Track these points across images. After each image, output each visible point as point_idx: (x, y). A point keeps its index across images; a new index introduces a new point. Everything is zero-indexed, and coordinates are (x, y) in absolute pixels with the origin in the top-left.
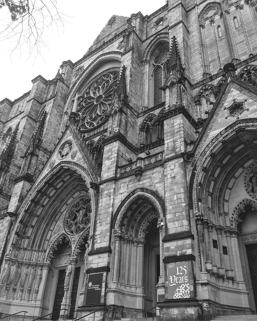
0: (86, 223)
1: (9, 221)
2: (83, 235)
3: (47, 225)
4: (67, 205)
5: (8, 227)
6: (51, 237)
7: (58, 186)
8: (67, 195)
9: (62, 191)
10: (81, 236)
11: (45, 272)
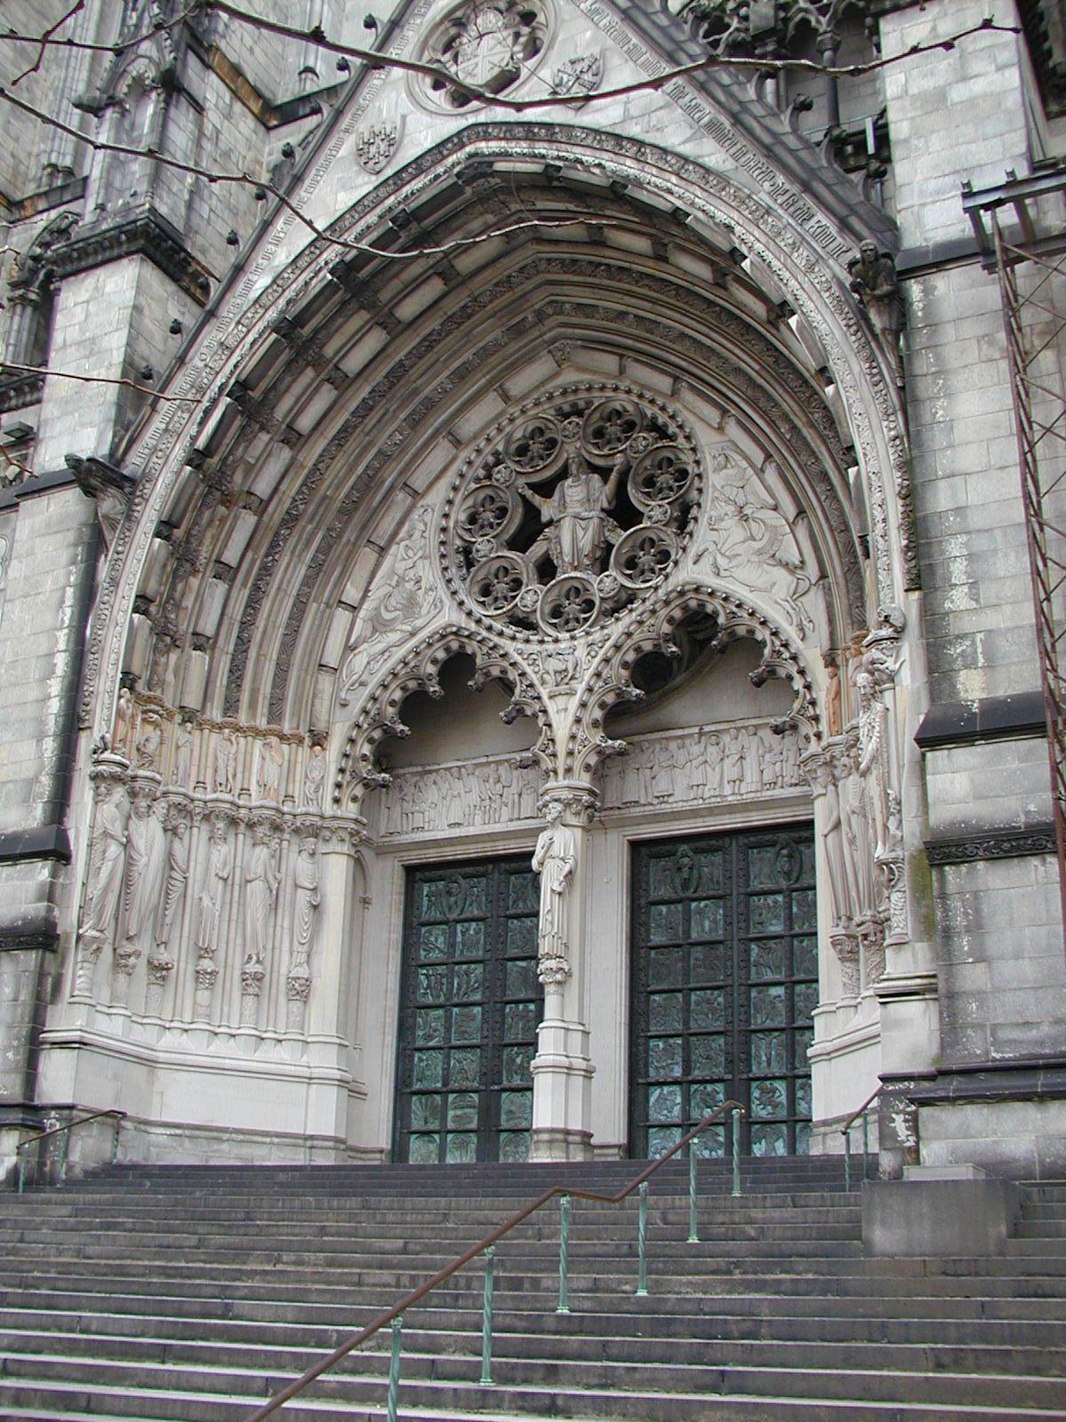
0: (631, 563)
1: (75, 525)
2: (630, 642)
3: (317, 568)
4: (457, 443)
5: (73, 563)
6: (350, 648)
7: (407, 310)
8: (461, 375)
9: (430, 343)
10: (617, 647)
11: (337, 869)
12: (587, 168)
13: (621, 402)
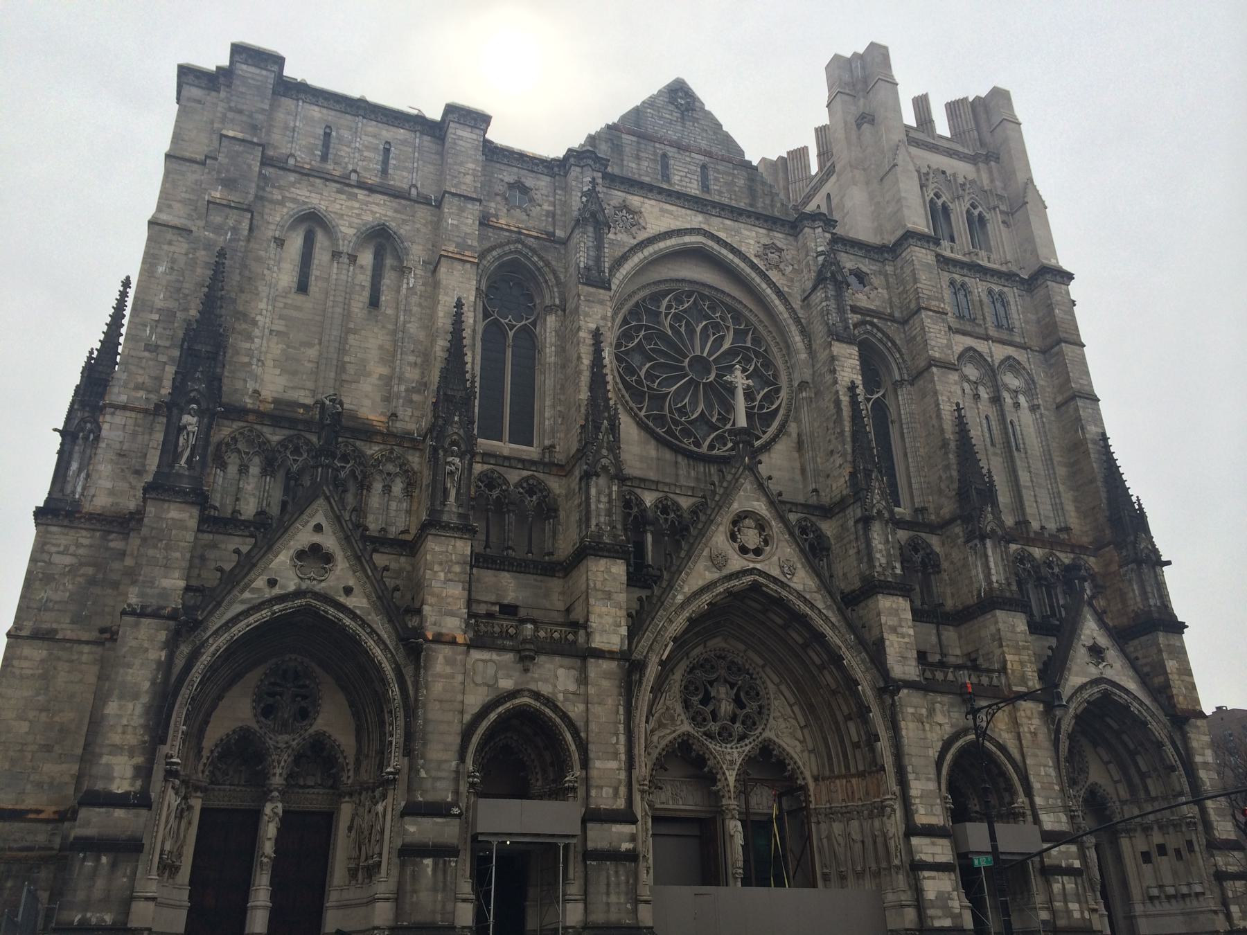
0: (743, 723)
12: (794, 604)
13: (739, 660)
